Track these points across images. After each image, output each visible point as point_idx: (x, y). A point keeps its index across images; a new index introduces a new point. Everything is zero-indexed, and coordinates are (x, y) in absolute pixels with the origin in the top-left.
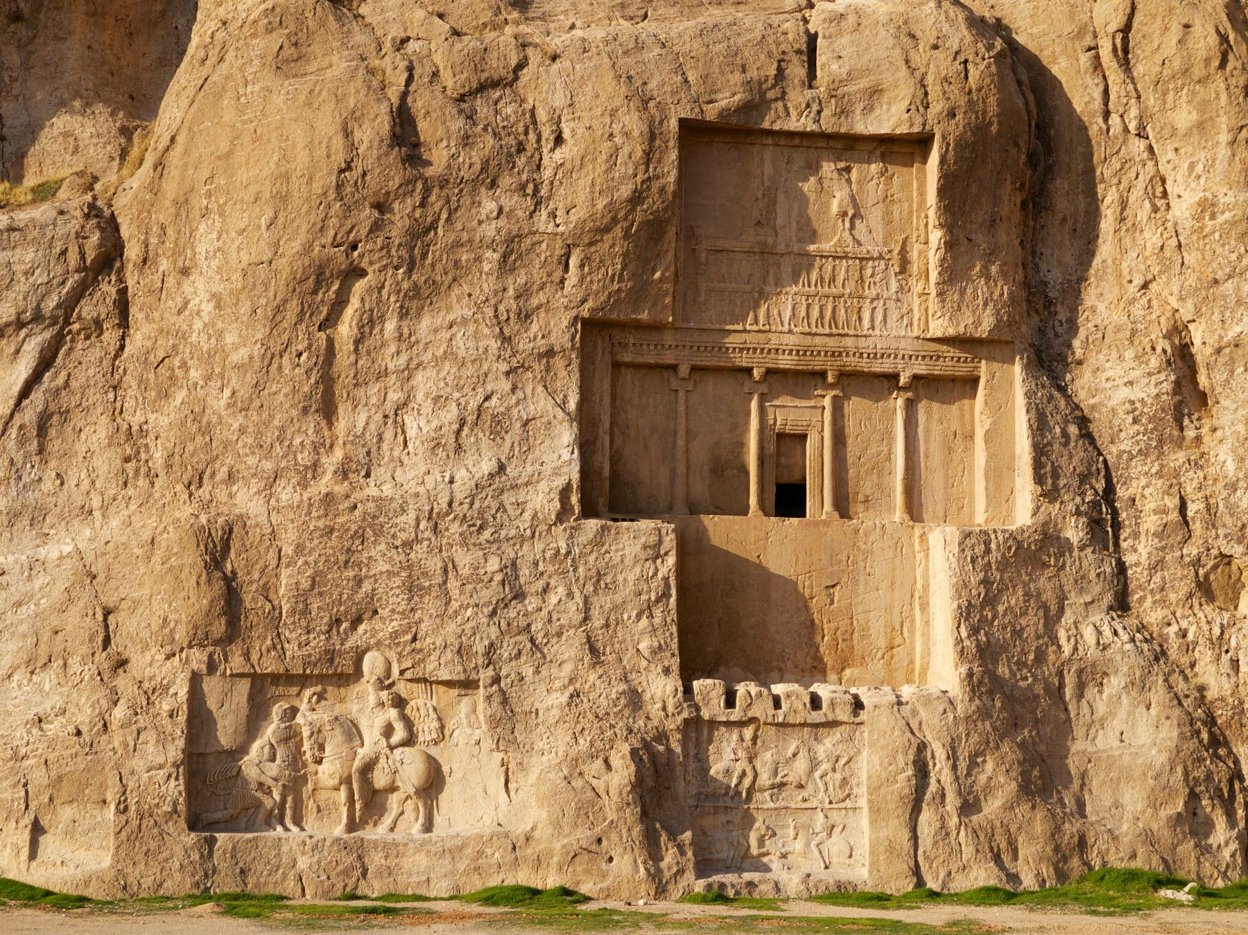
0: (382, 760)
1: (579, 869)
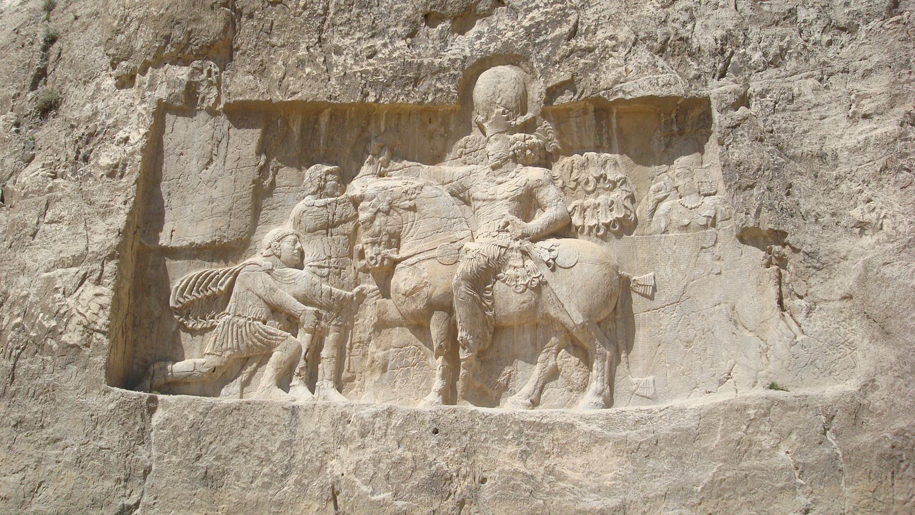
0: (515, 260)
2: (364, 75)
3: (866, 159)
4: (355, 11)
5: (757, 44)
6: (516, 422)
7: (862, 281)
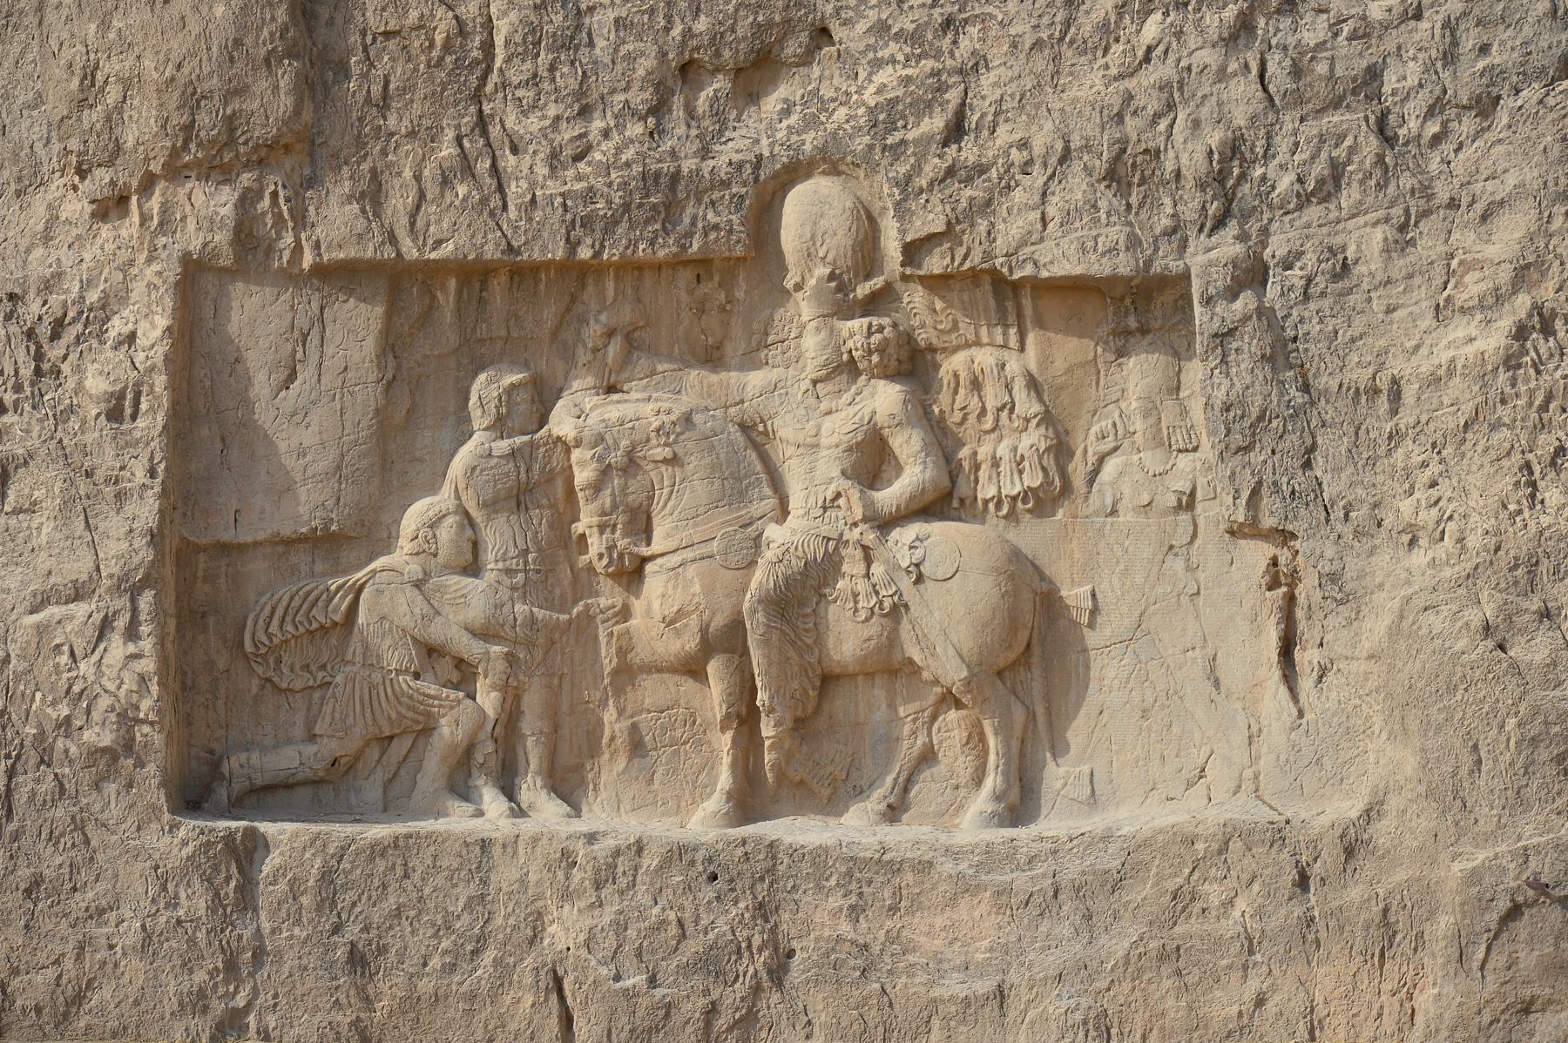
0: (852, 565)
2: (569, 203)
3: (1446, 401)
4: (544, 58)
5: (1288, 156)
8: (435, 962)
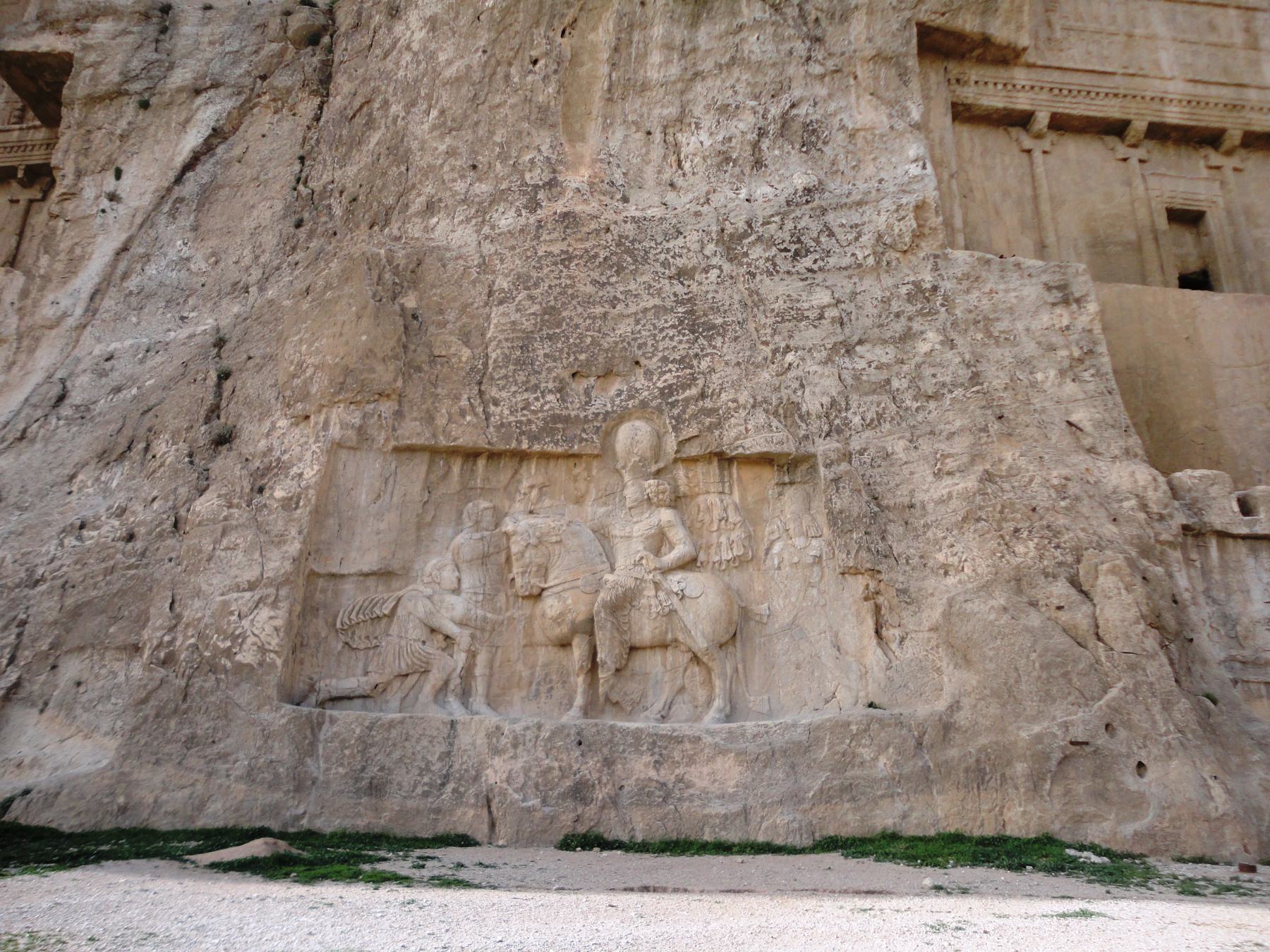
1: (1080, 788)
6: (649, 735)
7: (947, 615)
8: (419, 790)
